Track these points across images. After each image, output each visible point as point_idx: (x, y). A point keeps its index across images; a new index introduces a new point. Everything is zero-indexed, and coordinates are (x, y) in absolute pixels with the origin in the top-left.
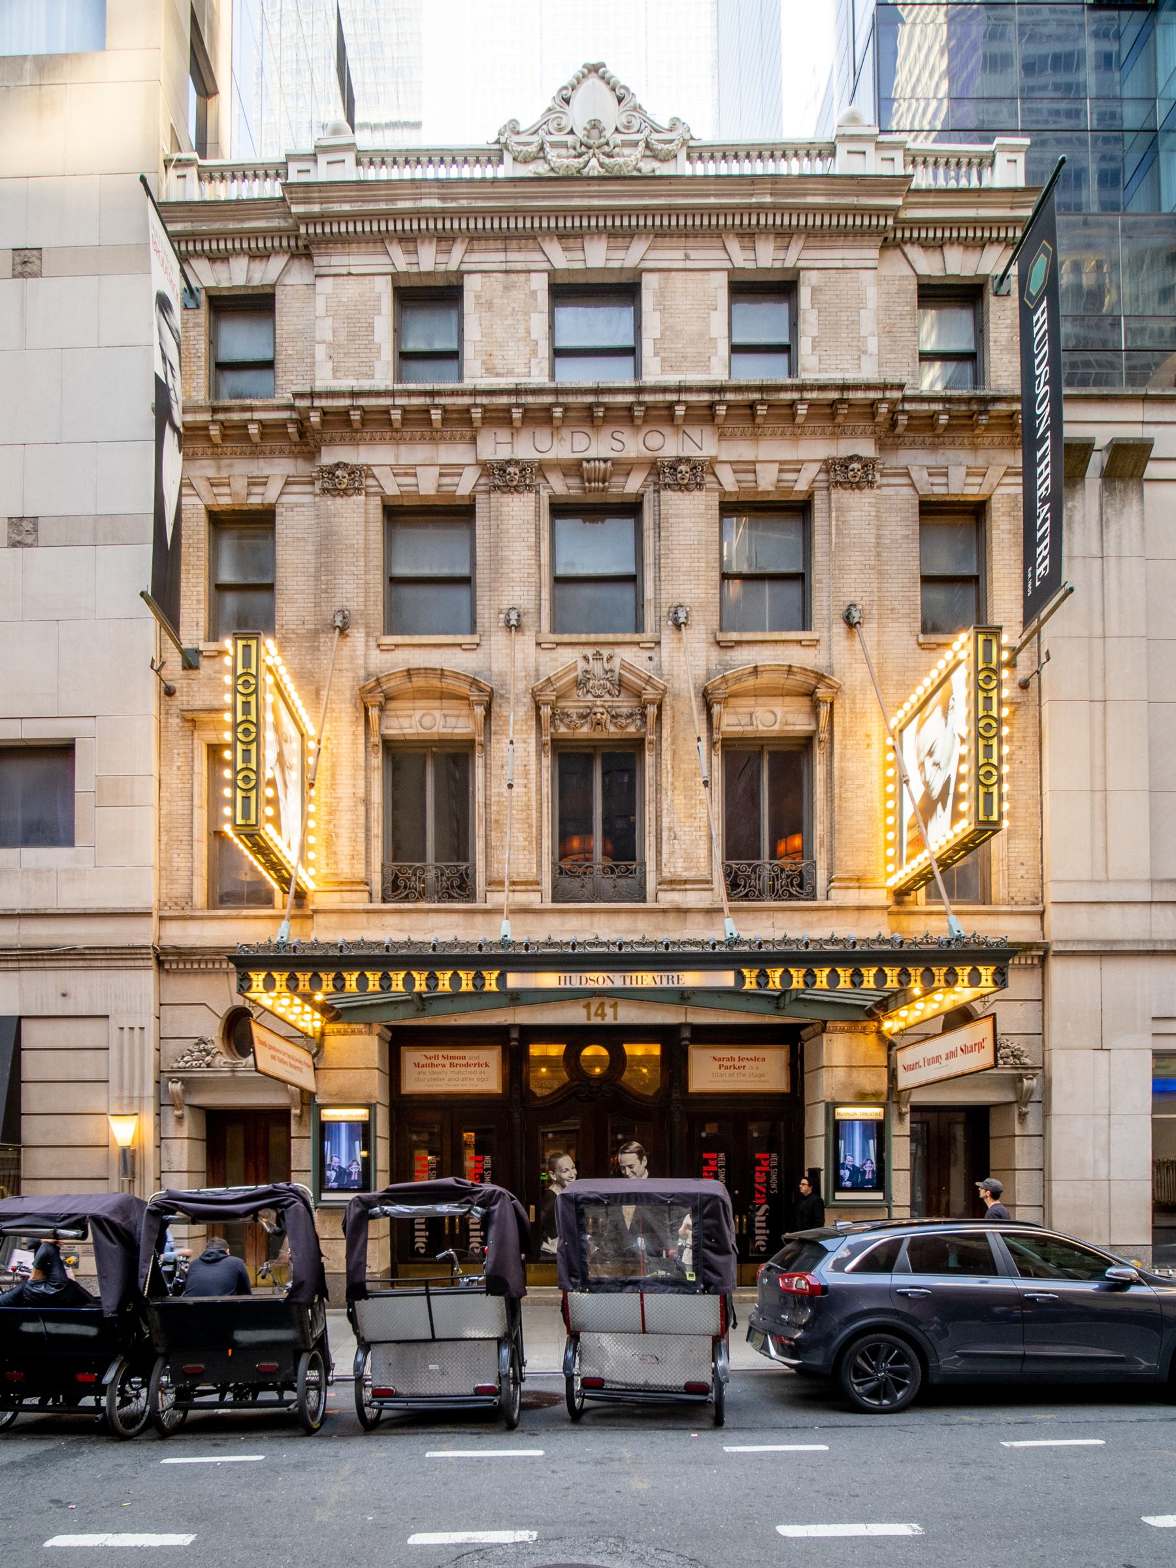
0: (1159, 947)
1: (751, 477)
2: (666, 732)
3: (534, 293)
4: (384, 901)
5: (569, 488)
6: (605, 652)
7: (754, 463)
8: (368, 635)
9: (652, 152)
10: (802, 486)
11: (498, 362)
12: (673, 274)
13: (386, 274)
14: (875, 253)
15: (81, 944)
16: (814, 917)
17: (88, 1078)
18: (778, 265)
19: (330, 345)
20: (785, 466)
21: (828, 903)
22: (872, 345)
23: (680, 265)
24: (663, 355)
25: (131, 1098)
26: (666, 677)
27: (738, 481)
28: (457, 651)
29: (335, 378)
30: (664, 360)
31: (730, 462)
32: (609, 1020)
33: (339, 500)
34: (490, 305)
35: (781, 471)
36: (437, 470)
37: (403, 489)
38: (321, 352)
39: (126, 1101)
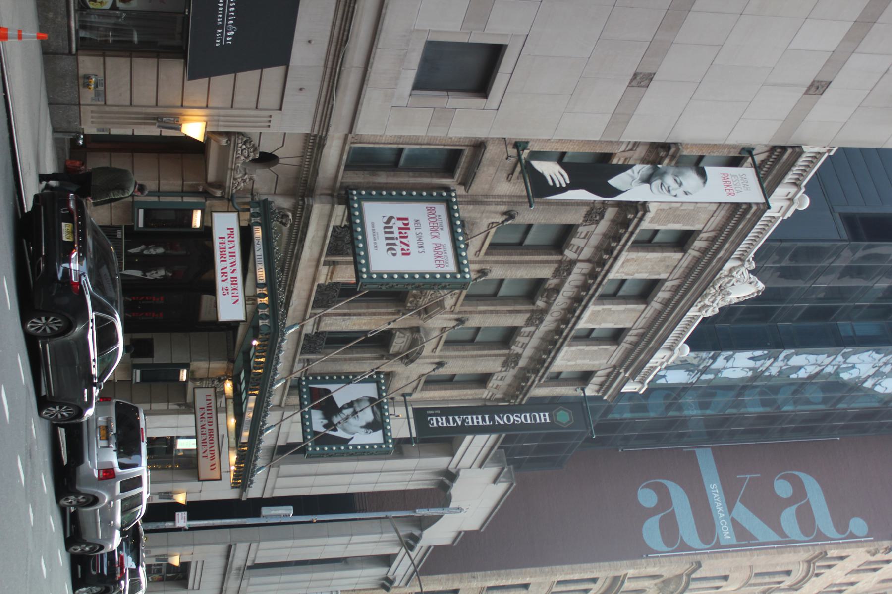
3: (659, 274)
7: (531, 337)
10: (513, 347)
14: (613, 363)
15: (336, 104)
16: (291, 359)
17: (237, 98)
21: (297, 360)
23: (643, 315)
25: (218, 121)
28: (478, 249)
31: (534, 332)
39: (216, 118)
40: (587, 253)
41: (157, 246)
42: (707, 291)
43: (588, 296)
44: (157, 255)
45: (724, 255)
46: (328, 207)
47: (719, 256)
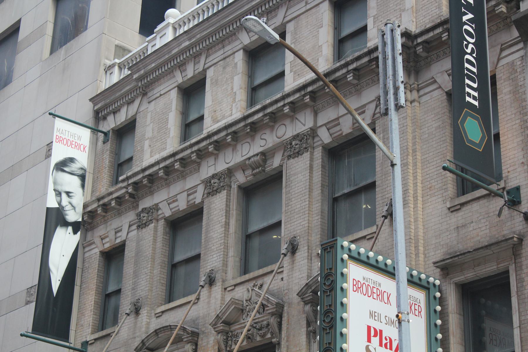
1: (338, 128)
5: (246, 177)
6: (259, 282)
7: (338, 119)
12: (301, 16)
13: (175, 88)
19: (151, 139)
24: (294, 70)
26: (286, 291)
27: (331, 135)
29: (151, 157)
30: (295, 73)
31: (325, 125)
33: (144, 230)
34: (217, 81)
36: (186, 192)
37: (173, 210)
43: (230, 130)
45: (184, 41)
47: (187, 43)
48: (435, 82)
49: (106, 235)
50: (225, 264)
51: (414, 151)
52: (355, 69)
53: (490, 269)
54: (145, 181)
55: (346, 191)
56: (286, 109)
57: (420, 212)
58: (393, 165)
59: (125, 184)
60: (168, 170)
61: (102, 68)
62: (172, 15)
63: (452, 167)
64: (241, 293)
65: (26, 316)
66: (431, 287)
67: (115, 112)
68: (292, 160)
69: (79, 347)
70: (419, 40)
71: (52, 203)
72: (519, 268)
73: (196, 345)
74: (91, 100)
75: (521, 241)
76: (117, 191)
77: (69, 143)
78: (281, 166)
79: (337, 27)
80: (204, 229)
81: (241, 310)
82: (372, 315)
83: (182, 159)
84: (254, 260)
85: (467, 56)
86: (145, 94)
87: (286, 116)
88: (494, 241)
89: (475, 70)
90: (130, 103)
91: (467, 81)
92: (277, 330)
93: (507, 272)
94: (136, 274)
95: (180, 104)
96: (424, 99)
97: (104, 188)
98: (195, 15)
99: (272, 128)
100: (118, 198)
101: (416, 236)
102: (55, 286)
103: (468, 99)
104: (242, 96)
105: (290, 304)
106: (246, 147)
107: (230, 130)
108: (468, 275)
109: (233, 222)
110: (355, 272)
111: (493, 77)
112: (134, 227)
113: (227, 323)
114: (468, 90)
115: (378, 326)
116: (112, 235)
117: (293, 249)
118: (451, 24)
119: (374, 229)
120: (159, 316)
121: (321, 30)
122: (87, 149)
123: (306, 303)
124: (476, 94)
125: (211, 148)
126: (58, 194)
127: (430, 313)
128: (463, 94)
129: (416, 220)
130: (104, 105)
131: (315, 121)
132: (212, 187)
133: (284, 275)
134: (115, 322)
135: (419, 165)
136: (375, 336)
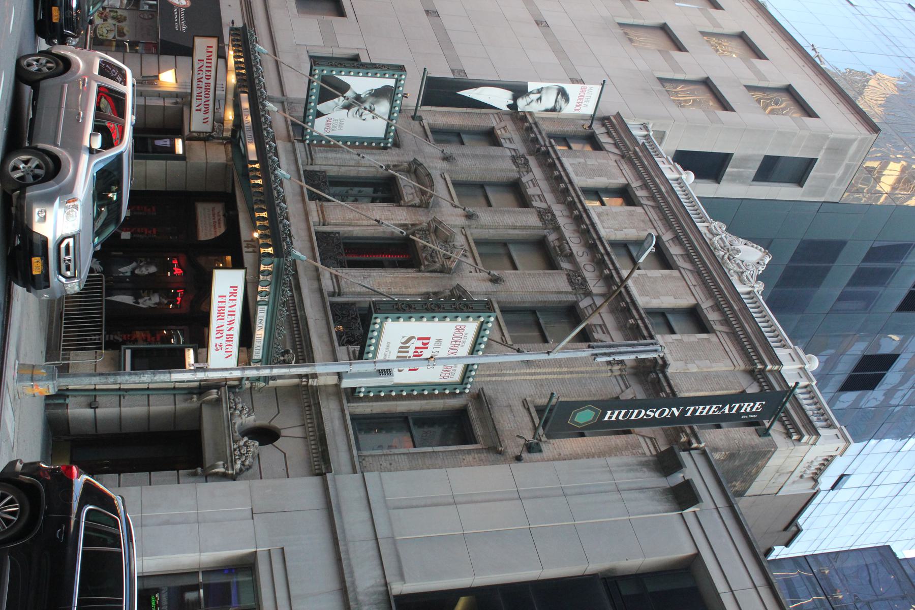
0: (341, 543)
1: (591, 312)
2: (428, 274)
4: (305, 171)
6: (468, 254)
8: (448, 171)
9: (740, 275)
11: (605, 217)
14: (743, 367)
16: (326, 339)
18: (712, 323)
19: (585, 163)
20: (603, 327)
22: (693, 368)
23: (689, 283)
31: (594, 303)
32: (245, 250)
35: (600, 325)
38: (582, 160)
40: (549, 197)
41: (149, 264)
42: (717, 253)
43: (590, 227)
44: (150, 275)
45: (665, 188)
46: (289, 144)
47: (664, 190)
48: (627, 388)
49: (508, 132)
50: (482, 227)
51: (572, 373)
52: (638, 325)
53: (478, 430)
54: (550, 160)
55: (541, 321)
56: (606, 272)
57: (522, 378)
58: (548, 353)
59: (548, 144)
60: (559, 179)
61: (645, 121)
62: (689, 177)
63: (554, 400)
64: (460, 240)
65: (442, 71)
66: (464, 386)
67: (608, 133)
68: (565, 277)
69: (418, 114)
70: (660, 375)
71: (532, 86)
72: (478, 451)
73: (419, 207)
74: (618, 113)
75: (500, 453)
76: (543, 138)
77: (581, 98)
78: (561, 269)
79: (675, 311)
80: (511, 209)
81: (447, 241)
82: (439, 341)
83: (567, 189)
84: (485, 250)
85: (643, 412)
86: (623, 156)
87: (601, 272)
88: (500, 433)
89: (633, 417)
90: (616, 145)
91: (623, 412)
92: (431, 269)
93: (476, 443)
94: (475, 156)
95: (614, 186)
96: (614, 380)
97: (546, 127)
98: (688, 195)
99: (592, 260)
100: (537, 139)
101: (504, 375)
102: (465, 93)
103: (609, 412)
104: (620, 236)
105: (451, 279)
106: (577, 240)
107: (590, 227)
108: (473, 414)
109: (516, 232)
110: (471, 327)
111: (629, 432)
112: (513, 153)
113: (436, 229)
114: (617, 412)
115: (430, 346)
116: (508, 135)
117: (495, 280)
118: (674, 400)
119: (510, 342)
120: (442, 176)
121: (672, 298)
122: (577, 112)
123: (451, 291)
124: (613, 418)
125: (576, 212)
126: (539, 91)
127: (444, 386)
128: (613, 409)
129: (516, 374)
130: (614, 124)
131: (597, 295)
132: (545, 215)
133: (474, 274)
134: (438, 141)
135: (561, 376)
136: (423, 344)
